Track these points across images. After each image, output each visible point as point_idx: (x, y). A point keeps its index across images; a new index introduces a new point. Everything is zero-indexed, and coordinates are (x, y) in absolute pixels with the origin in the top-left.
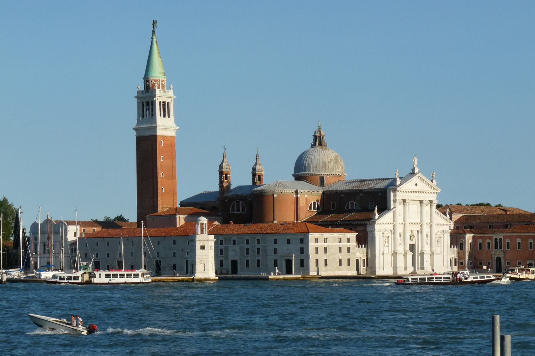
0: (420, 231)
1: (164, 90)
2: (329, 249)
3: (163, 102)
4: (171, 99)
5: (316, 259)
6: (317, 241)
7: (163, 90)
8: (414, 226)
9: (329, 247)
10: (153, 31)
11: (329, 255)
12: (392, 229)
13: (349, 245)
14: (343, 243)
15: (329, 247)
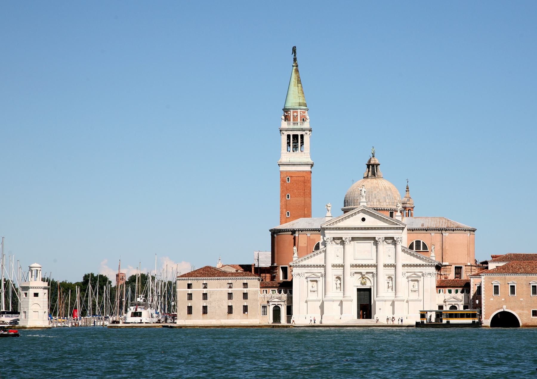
0: (375, 272)
1: (297, 122)
2: (211, 294)
3: (294, 136)
4: (305, 132)
5: (188, 307)
6: (189, 286)
7: (295, 122)
8: (364, 268)
9: (211, 293)
10: (295, 60)
11: (210, 301)
12: (323, 272)
13: (245, 290)
14: (235, 288)
15: (210, 292)
